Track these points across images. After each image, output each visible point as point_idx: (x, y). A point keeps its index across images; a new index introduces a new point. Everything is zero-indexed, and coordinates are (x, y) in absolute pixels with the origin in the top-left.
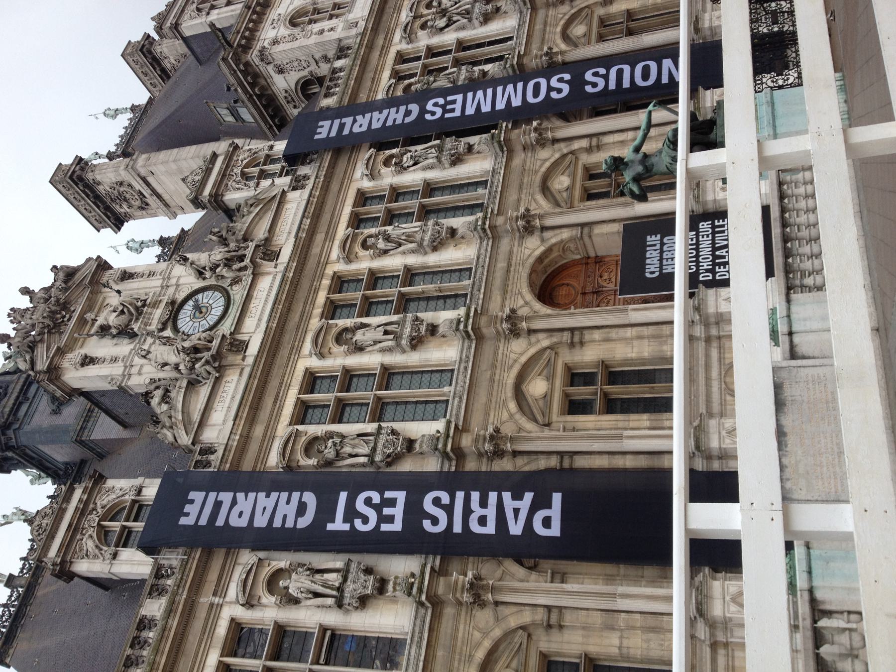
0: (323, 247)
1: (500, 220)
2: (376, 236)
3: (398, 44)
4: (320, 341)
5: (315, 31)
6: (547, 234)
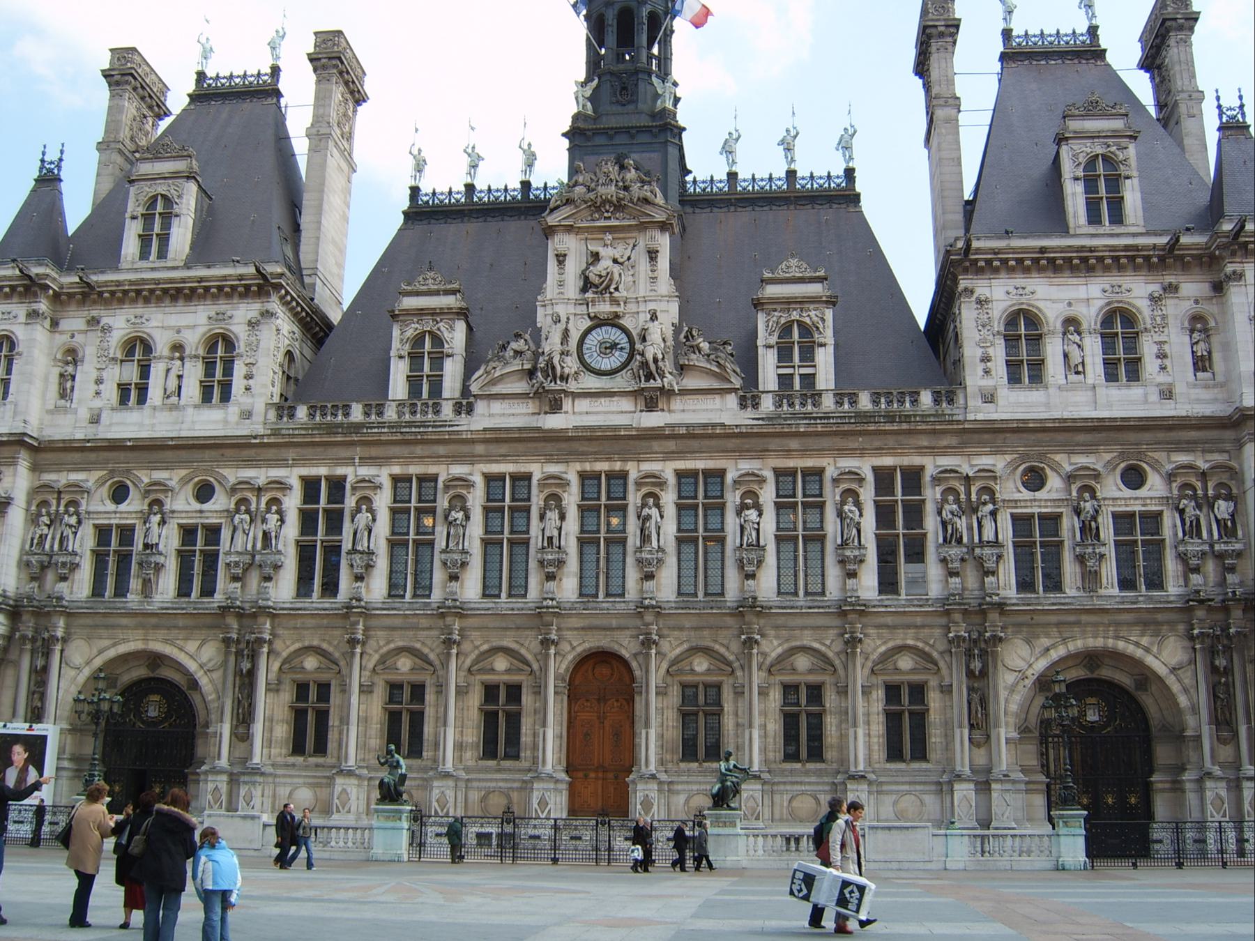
0: (657, 453)
1: (649, 618)
2: (658, 506)
3: (931, 465)
4: (549, 481)
5: (991, 351)
6: (641, 658)
